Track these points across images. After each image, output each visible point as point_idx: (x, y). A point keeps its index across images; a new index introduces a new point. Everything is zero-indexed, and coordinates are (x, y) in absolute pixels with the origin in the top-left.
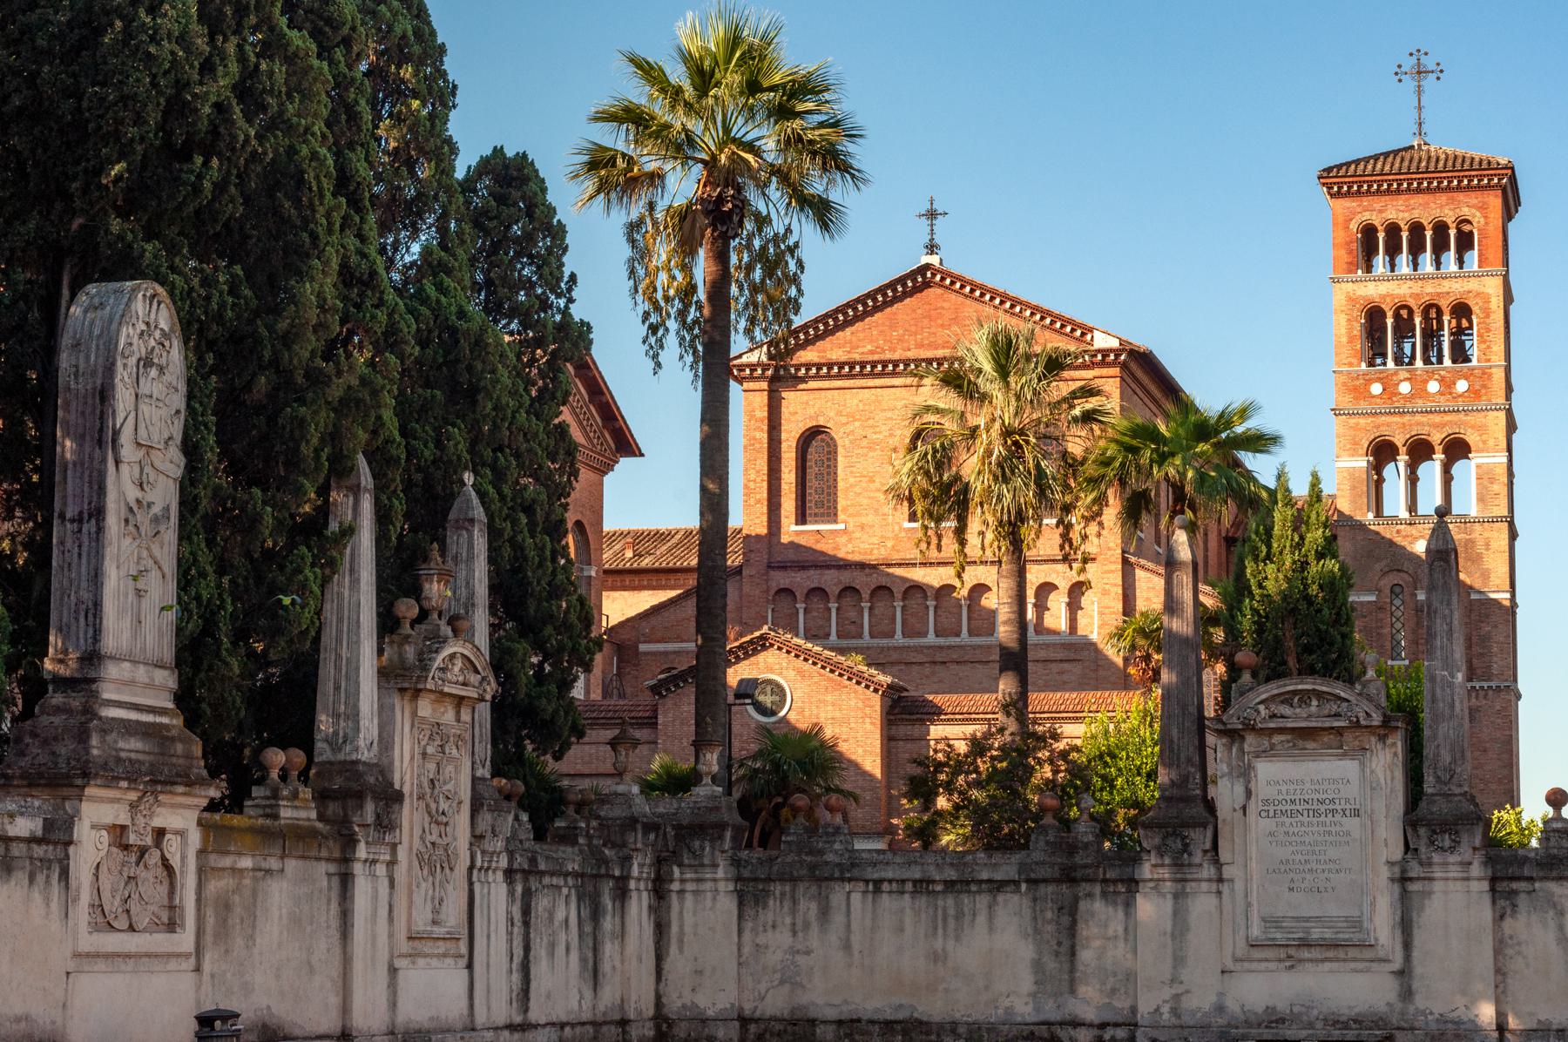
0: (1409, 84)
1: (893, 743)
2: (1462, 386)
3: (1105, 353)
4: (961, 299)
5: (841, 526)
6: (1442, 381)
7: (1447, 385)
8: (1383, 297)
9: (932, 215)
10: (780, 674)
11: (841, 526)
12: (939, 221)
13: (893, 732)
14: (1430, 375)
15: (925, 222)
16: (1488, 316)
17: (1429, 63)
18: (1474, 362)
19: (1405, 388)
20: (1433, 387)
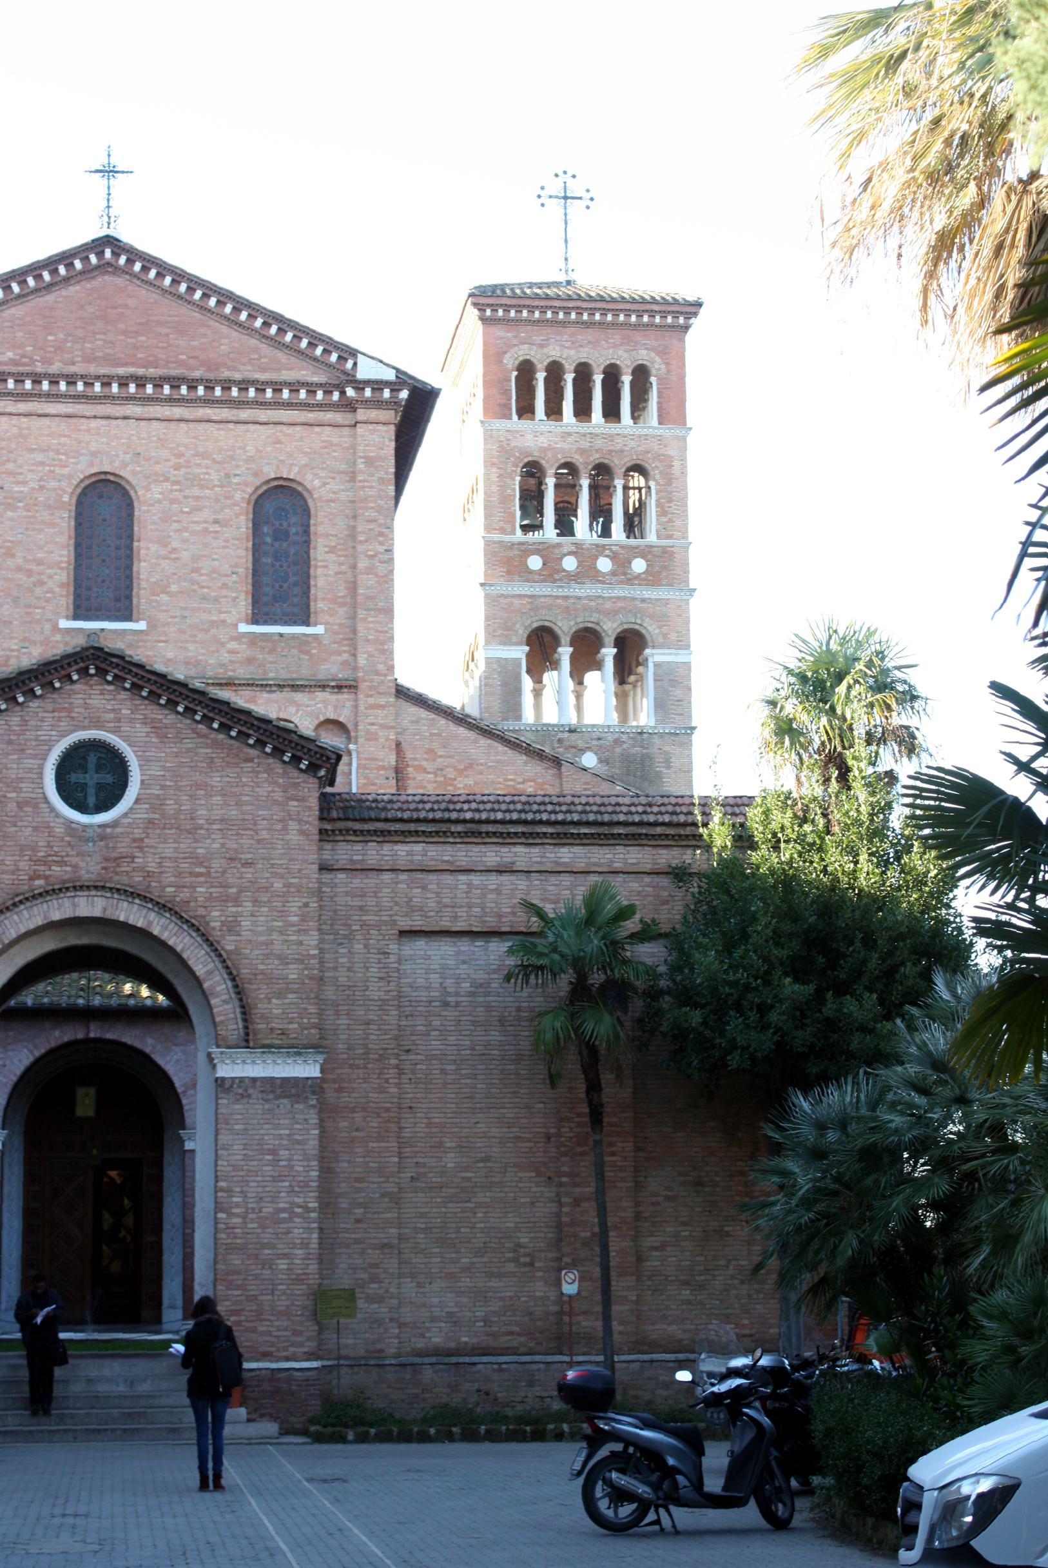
0: (555, 206)
1: (327, 877)
2: (639, 566)
3: (378, 385)
4: (155, 296)
6: (614, 557)
7: (621, 561)
8: (544, 450)
9: (109, 171)
10: (116, 731)
13: (326, 855)
14: (600, 550)
15: (99, 181)
16: (669, 483)
18: (652, 538)
20: (604, 564)
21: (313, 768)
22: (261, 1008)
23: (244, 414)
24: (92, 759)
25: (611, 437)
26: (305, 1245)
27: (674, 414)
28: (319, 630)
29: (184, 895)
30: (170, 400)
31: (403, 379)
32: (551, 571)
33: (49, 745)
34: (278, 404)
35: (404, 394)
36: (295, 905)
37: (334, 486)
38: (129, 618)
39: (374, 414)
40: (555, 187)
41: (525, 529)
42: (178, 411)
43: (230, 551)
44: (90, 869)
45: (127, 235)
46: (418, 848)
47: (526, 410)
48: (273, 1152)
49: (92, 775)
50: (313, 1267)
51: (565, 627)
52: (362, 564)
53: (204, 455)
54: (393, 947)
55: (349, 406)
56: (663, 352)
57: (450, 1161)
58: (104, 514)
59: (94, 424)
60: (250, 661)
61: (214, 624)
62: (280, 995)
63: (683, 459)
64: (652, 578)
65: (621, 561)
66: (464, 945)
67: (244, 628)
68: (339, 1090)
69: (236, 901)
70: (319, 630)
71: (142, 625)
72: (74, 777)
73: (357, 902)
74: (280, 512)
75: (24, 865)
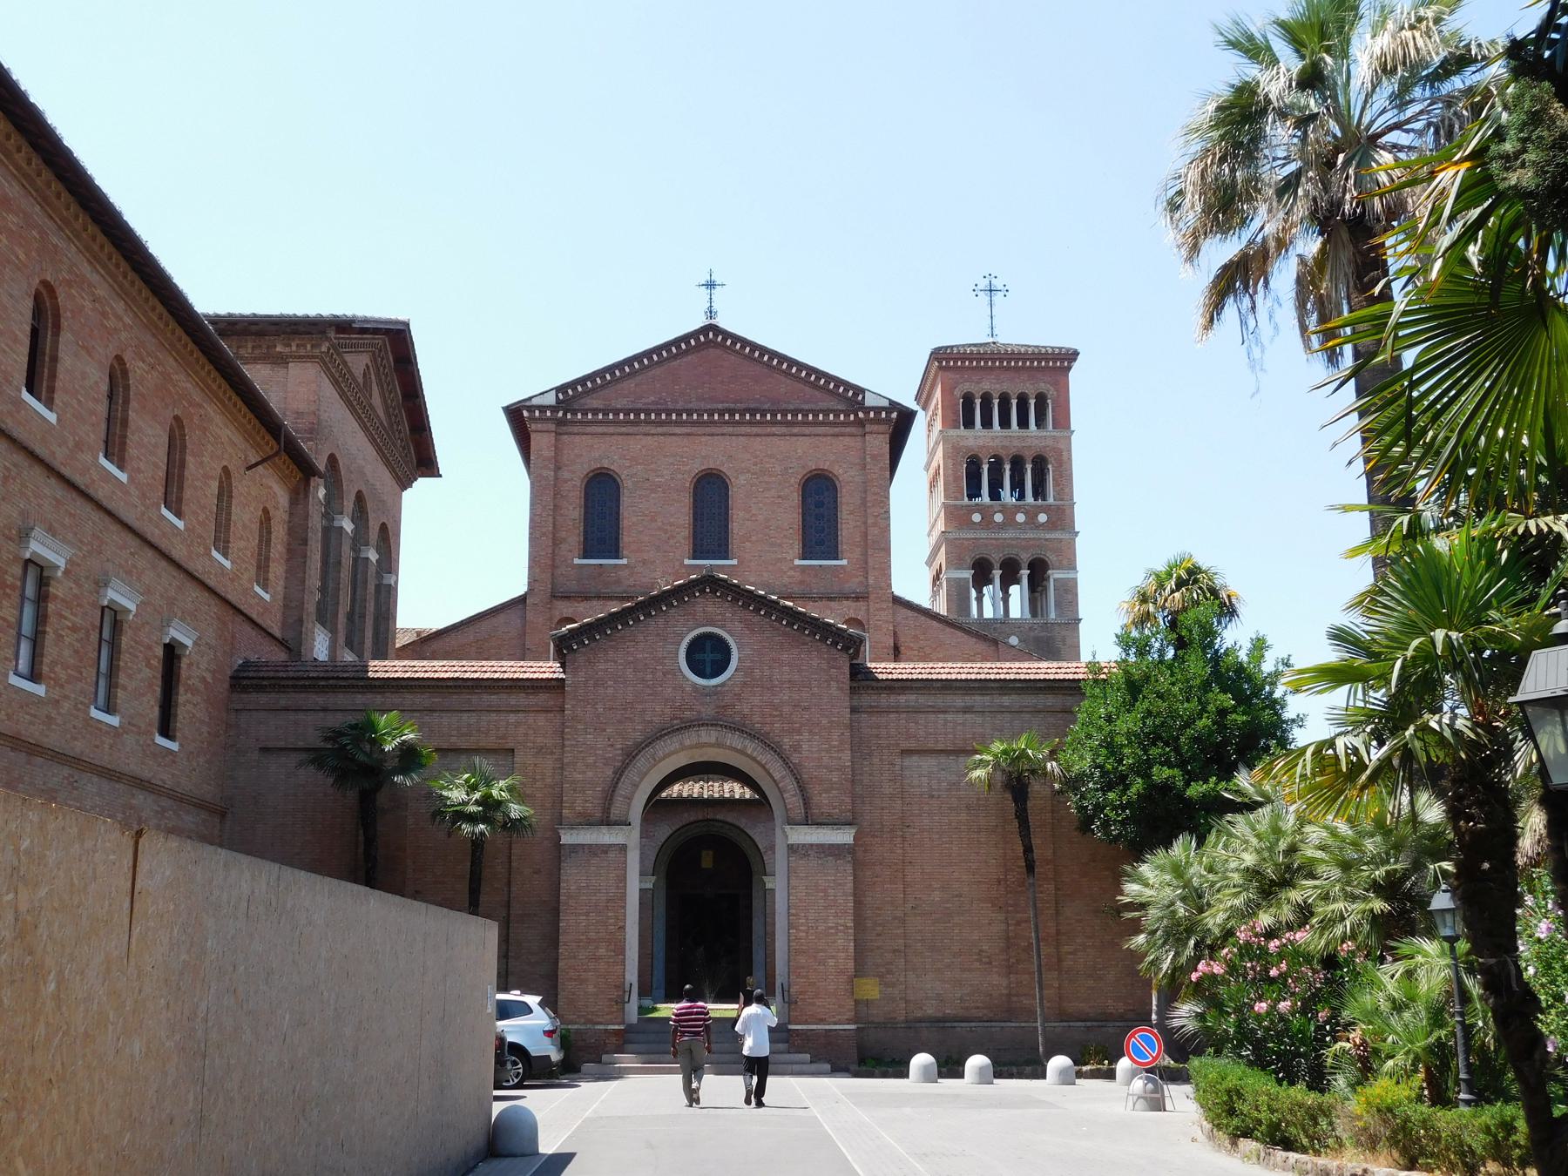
2: (1042, 518)
3: (878, 410)
5: (625, 561)
7: (1031, 515)
9: (711, 285)
10: (722, 627)
11: (625, 561)
12: (717, 291)
14: (1017, 509)
17: (998, 284)
18: (1051, 500)
19: (998, 518)
20: (1020, 518)
21: (845, 649)
22: (815, 800)
23: (796, 430)
24: (708, 644)
25: (1023, 438)
26: (846, 950)
27: (1063, 422)
28: (844, 562)
29: (767, 728)
30: (750, 423)
31: (894, 405)
32: (988, 522)
33: (682, 637)
34: (816, 423)
35: (894, 415)
36: (835, 735)
37: (852, 472)
38: (726, 558)
39: (875, 428)
40: (983, 284)
41: (970, 497)
42: (755, 430)
43: (788, 515)
44: (708, 711)
45: (723, 322)
46: (913, 697)
47: (969, 423)
48: (825, 891)
49: (708, 655)
50: (851, 964)
51: (996, 558)
52: (870, 521)
53: (771, 456)
54: (898, 761)
55: (860, 423)
56: (1055, 384)
57: (937, 896)
58: (710, 492)
59: (704, 439)
60: (801, 582)
61: (779, 560)
62: (827, 791)
63: (1069, 451)
64: (1052, 525)
65: (1031, 515)
66: (943, 759)
67: (797, 562)
68: (865, 851)
69: (799, 732)
70: (844, 562)
71: (734, 562)
72: (699, 656)
73: (875, 732)
74: (819, 492)
75: (667, 711)
